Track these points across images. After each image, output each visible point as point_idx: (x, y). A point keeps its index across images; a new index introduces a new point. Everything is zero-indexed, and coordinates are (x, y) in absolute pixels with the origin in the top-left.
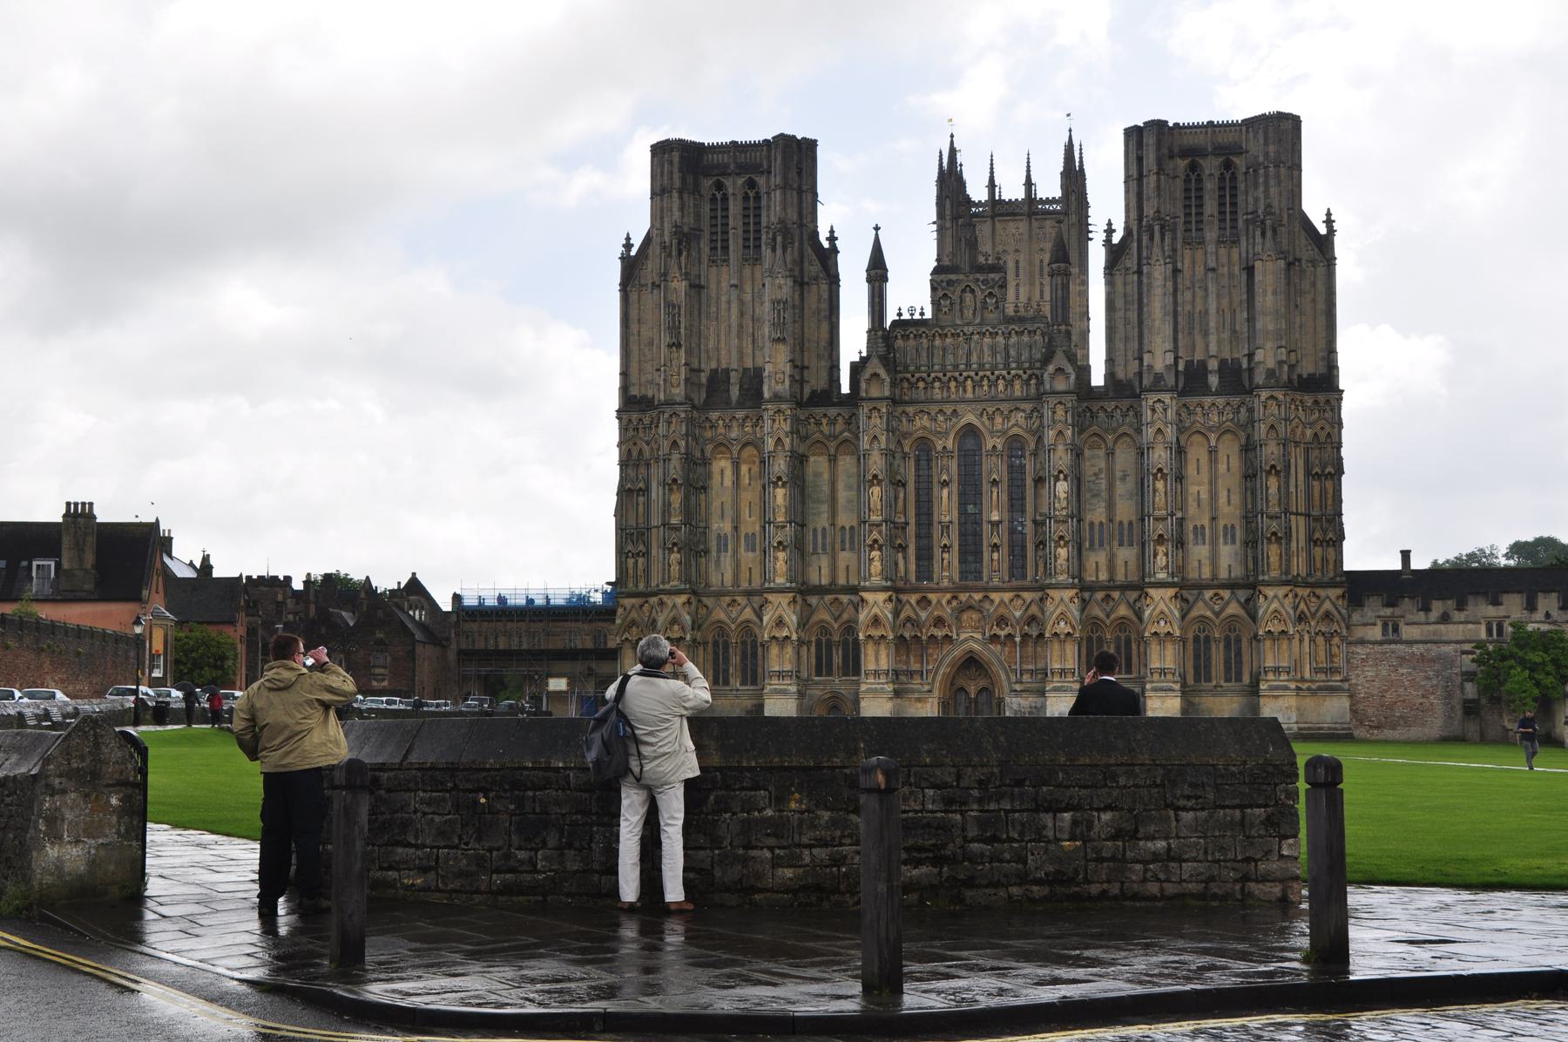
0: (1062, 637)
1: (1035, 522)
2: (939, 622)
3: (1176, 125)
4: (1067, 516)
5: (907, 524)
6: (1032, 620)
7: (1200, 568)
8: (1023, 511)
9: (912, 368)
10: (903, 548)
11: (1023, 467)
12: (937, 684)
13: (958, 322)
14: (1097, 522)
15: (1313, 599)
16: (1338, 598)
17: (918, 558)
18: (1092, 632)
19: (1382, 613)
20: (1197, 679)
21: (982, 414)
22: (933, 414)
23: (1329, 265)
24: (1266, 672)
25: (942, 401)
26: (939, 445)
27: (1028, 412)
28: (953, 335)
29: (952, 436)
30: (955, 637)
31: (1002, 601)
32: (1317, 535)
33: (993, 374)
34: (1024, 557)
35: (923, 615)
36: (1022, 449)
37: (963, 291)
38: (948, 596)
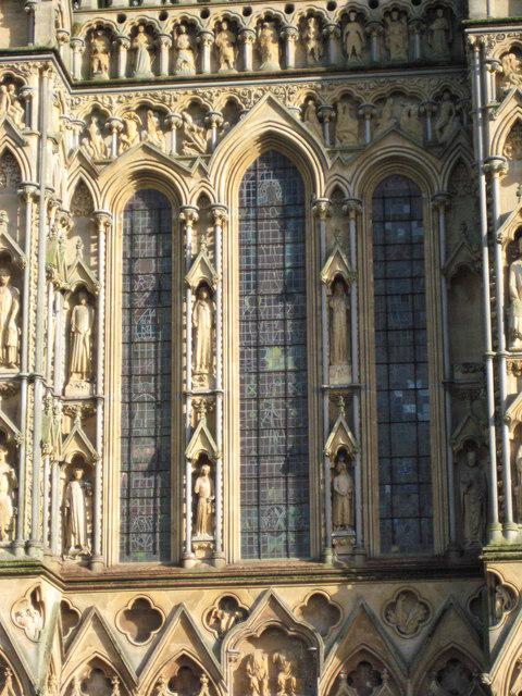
1: (450, 386)
5: (94, 400)
6: (454, 658)
8: (418, 363)
10: (83, 467)
11: (415, 244)
21: (304, 107)
22: (176, 111)
25: (200, 78)
26: (190, 190)
27: (427, 97)
31: (363, 609)
34: (424, 484)
35: (134, 653)
36: (413, 197)
38: (211, 597)
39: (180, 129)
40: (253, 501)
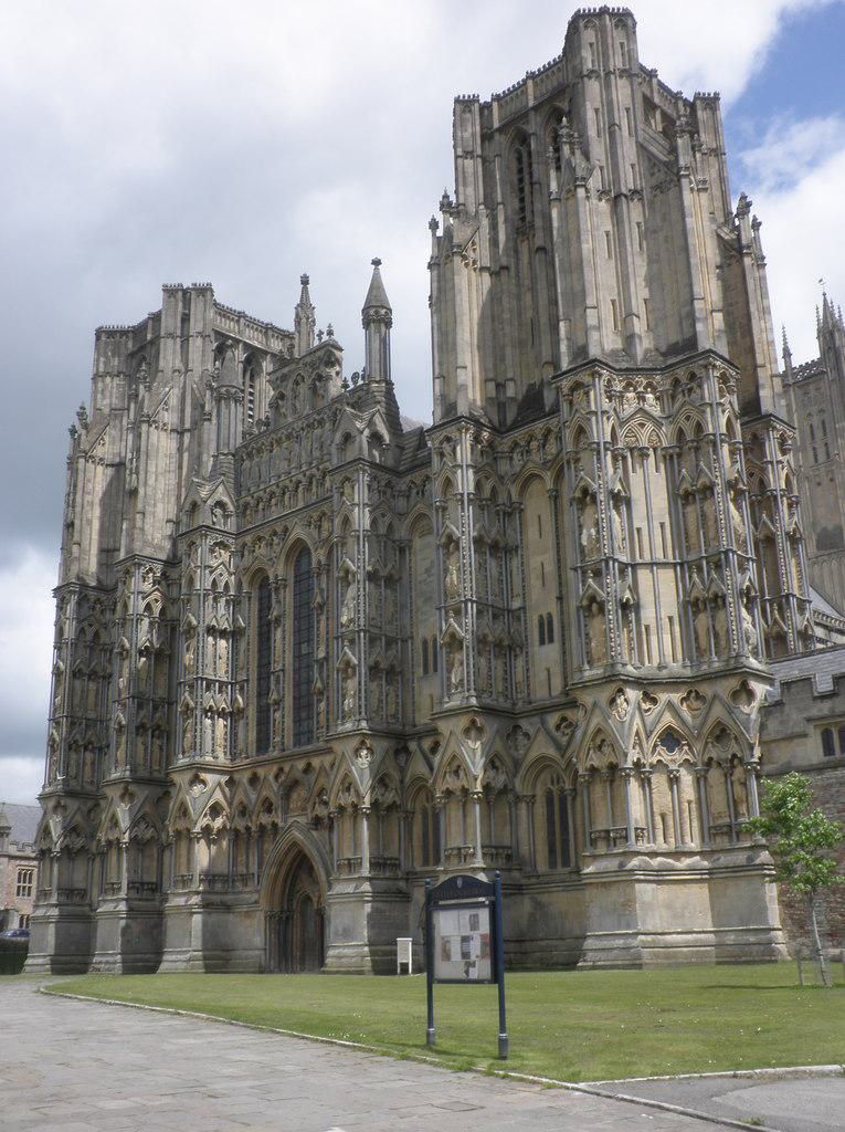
0: (350, 810)
2: (268, 807)
3: (497, 98)
4: (353, 632)
7: (549, 679)
9: (253, 490)
12: (263, 893)
13: (290, 420)
14: (429, 637)
15: (696, 704)
16: (735, 695)
17: (259, 723)
18: (428, 802)
19: (814, 712)
20: (552, 864)
23: (679, 180)
24: (593, 842)
28: (289, 437)
29: (283, 558)
30: (280, 824)
31: (322, 768)
32: (699, 592)
33: (318, 469)
37: (298, 384)
38: (275, 768)
39: (271, 544)
40: (297, 721)
